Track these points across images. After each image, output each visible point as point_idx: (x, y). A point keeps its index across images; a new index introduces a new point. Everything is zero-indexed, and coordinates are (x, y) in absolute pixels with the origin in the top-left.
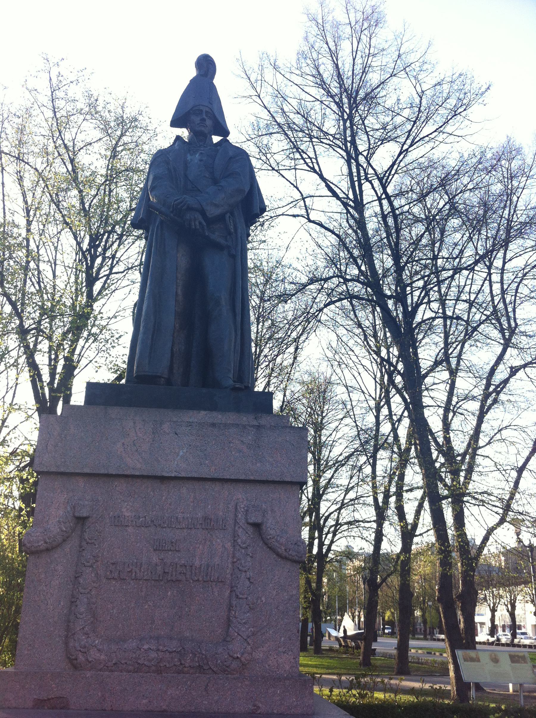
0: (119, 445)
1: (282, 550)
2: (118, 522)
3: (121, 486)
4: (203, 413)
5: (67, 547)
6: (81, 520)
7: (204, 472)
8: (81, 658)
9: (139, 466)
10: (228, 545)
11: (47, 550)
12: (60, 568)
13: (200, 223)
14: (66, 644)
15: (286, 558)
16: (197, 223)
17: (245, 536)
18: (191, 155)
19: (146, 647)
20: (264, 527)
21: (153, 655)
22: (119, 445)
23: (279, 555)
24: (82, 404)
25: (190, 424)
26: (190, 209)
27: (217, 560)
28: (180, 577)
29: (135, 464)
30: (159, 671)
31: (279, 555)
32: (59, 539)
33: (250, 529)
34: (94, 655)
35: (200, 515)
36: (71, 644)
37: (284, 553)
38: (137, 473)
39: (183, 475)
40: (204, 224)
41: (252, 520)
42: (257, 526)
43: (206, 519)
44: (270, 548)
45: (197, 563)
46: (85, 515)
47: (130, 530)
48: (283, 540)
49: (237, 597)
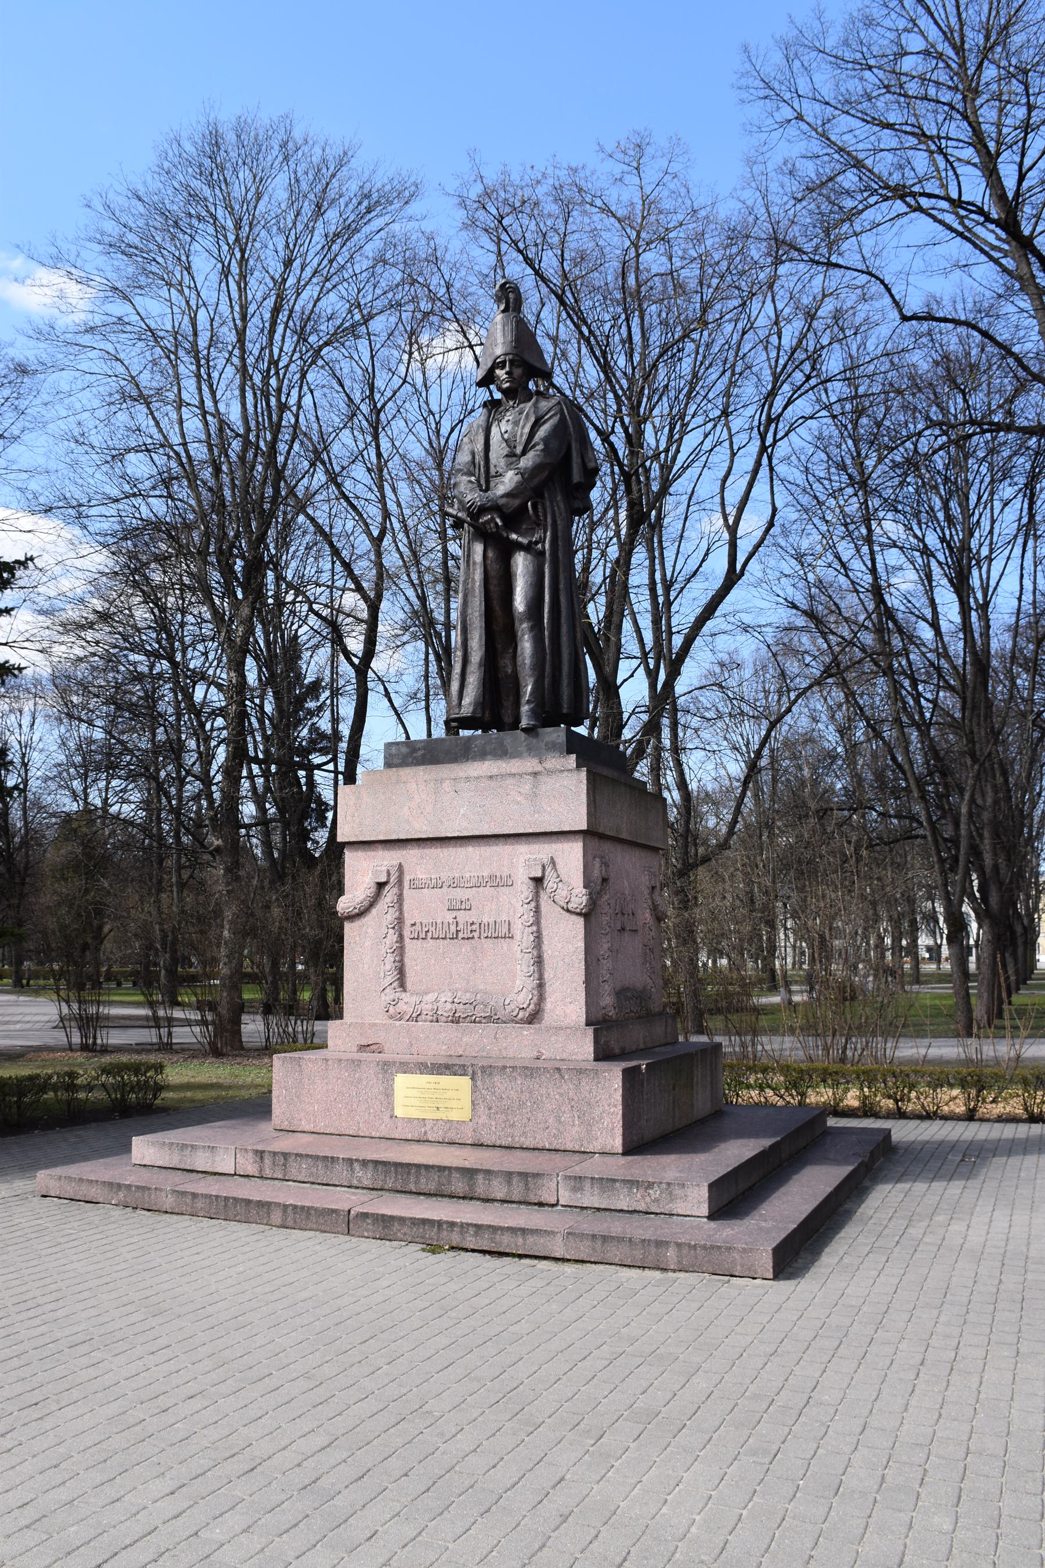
0: (406, 809)
4: (487, 763)
6: (381, 886)
21: (449, 1006)
22: (406, 809)
27: (504, 918)
33: (531, 884)
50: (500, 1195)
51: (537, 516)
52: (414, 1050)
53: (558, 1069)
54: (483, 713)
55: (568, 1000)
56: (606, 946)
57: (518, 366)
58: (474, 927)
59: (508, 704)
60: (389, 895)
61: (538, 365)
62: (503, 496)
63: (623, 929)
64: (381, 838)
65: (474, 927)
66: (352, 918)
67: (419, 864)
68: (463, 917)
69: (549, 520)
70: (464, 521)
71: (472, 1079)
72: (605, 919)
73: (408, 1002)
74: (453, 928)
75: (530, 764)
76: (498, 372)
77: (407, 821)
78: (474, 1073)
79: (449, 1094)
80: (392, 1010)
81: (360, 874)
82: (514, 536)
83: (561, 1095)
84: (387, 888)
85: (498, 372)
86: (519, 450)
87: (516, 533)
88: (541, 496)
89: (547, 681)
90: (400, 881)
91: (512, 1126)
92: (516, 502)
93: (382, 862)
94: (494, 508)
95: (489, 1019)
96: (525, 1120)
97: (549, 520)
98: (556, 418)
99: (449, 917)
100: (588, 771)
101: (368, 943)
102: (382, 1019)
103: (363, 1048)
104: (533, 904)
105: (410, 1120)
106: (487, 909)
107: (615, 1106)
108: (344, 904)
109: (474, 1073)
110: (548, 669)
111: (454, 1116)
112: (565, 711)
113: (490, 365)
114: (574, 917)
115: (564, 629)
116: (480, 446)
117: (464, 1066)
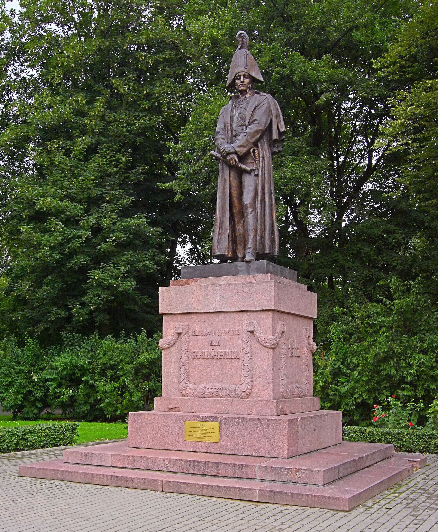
1: (263, 343)
3: (195, 317)
5: (176, 346)
6: (179, 334)
8: (184, 392)
10: (240, 342)
11: (169, 348)
12: (174, 355)
13: (235, 160)
15: (265, 347)
16: (234, 161)
17: (247, 337)
21: (210, 390)
23: (263, 345)
24: (160, 288)
25: (220, 285)
26: (228, 154)
27: (236, 349)
28: (221, 357)
31: (263, 345)
32: (172, 343)
33: (249, 334)
34: (188, 390)
37: (264, 344)
40: (237, 160)
42: (252, 332)
43: (230, 330)
45: (228, 351)
47: (200, 337)
48: (263, 338)
50: (230, 475)
51: (255, 156)
52: (194, 410)
53: (259, 419)
54: (228, 253)
55: (265, 388)
56: (283, 363)
57: (247, 78)
58: (222, 354)
59: (240, 248)
60: (183, 338)
62: (238, 147)
63: (293, 356)
65: (222, 354)
66: (165, 349)
67: (197, 325)
68: (216, 348)
69: (261, 159)
70: (220, 159)
71: (220, 423)
72: (283, 351)
74: (212, 354)
75: (249, 278)
76: (237, 81)
77: (192, 304)
78: (221, 421)
79: (209, 431)
80: (184, 392)
81: (169, 328)
82: (243, 166)
83: (260, 431)
84: (182, 335)
85: (237, 81)
86: (247, 123)
87: (244, 164)
88: (257, 146)
89: (258, 238)
90: (188, 332)
91: (238, 445)
92: (245, 150)
93: (180, 324)
96: (244, 442)
97: (261, 159)
98: (264, 107)
99: (211, 349)
100: (275, 282)
102: (179, 397)
106: (228, 345)
107: (284, 436)
108: (162, 342)
109: (221, 421)
110: (259, 232)
111: (211, 440)
112: (267, 252)
113: (233, 77)
114: (267, 350)
115: (267, 212)
117: (216, 417)
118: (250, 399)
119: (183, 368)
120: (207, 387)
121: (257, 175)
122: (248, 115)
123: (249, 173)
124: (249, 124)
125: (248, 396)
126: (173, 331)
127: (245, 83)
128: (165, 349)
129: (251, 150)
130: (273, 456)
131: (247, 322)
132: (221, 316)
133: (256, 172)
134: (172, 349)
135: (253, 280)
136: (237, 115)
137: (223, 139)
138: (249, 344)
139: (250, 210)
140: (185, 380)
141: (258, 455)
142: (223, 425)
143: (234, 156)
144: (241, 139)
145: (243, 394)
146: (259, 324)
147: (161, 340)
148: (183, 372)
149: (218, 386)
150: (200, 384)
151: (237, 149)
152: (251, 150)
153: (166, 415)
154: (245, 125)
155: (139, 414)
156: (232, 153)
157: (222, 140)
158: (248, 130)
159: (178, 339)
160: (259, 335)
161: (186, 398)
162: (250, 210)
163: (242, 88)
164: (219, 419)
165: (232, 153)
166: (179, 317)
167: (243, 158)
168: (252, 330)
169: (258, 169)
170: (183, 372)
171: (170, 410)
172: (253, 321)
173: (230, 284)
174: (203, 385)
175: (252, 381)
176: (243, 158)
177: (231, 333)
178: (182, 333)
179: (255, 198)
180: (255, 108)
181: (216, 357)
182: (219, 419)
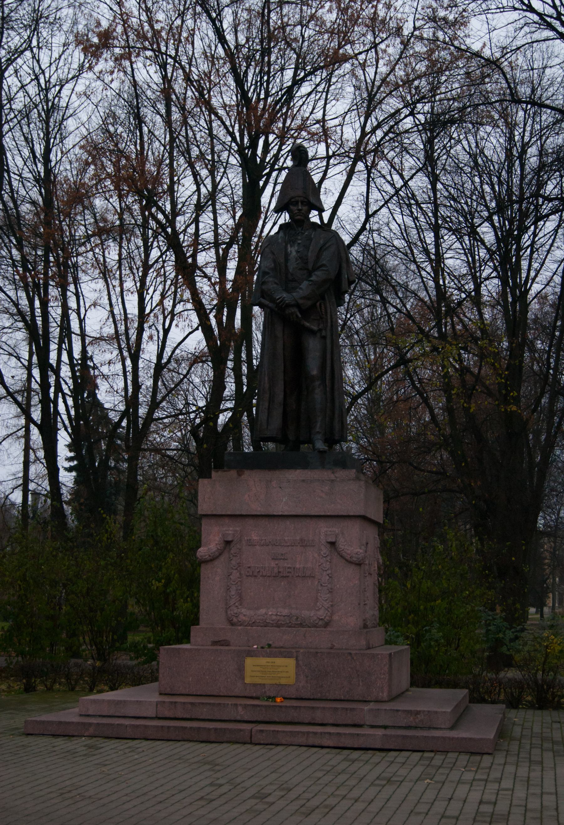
0: (246, 496)
1: (348, 557)
2: (250, 543)
3: (251, 521)
4: (298, 471)
5: (222, 558)
6: (228, 543)
7: (299, 512)
8: (235, 620)
9: (259, 509)
10: (316, 555)
12: (219, 570)
13: (297, 316)
14: (226, 612)
16: (294, 316)
17: (325, 550)
18: (291, 246)
19: (270, 613)
20: (337, 544)
21: (274, 617)
22: (246, 496)
23: (347, 560)
26: (288, 306)
27: (309, 565)
29: (257, 508)
30: (278, 626)
31: (347, 560)
32: (217, 554)
33: (329, 545)
34: (242, 618)
35: (298, 538)
36: (229, 613)
37: (349, 559)
38: (259, 513)
39: (286, 513)
40: (300, 316)
41: (330, 540)
42: (333, 544)
43: (302, 540)
44: (341, 556)
45: (298, 566)
46: (230, 539)
47: (258, 547)
48: (349, 552)
49: (321, 585)
53: (350, 654)
58: (289, 570)
61: (318, 205)
62: (301, 298)
64: (229, 513)
65: (289, 570)
66: (206, 562)
71: (297, 659)
73: (245, 614)
75: (326, 474)
82: (307, 324)
86: (310, 267)
88: (323, 298)
92: (309, 303)
93: (230, 529)
94: (298, 306)
95: (301, 625)
99: (273, 564)
101: (217, 578)
103: (215, 643)
104: (328, 558)
105: (255, 685)
107: (384, 674)
108: (202, 552)
111: (283, 681)
116: (282, 260)
118: (329, 629)
119: (234, 588)
120: (270, 613)
121: (324, 338)
122: (311, 256)
123: (313, 333)
124: (315, 269)
125: (327, 625)
126: (217, 538)
127: (303, 212)
128: (206, 562)
129: (318, 304)
130: (369, 699)
131: (325, 531)
132: (288, 522)
133: (324, 333)
134: (216, 563)
135: (332, 477)
136: (294, 253)
137: (276, 283)
138: (328, 558)
139: (317, 383)
140: (237, 604)
141: (349, 698)
142: (300, 662)
143: (295, 310)
144: (305, 288)
145: (320, 623)
146: (343, 534)
147: (199, 550)
148: (233, 593)
149: (285, 612)
150: (258, 608)
151: (301, 302)
152: (318, 304)
153: (217, 650)
154: (308, 269)
155: (176, 649)
156: (292, 306)
157: (275, 286)
158: (313, 278)
159: (225, 548)
160: (343, 547)
161: (240, 628)
162: (317, 383)
163: (299, 217)
164: (295, 654)
165: (292, 306)
166: (227, 520)
167: (306, 312)
168: (333, 540)
169: (326, 330)
170: (233, 593)
171: (215, 643)
172: (334, 529)
173: (303, 481)
174: (263, 611)
175: (332, 606)
176: (306, 312)
177: (304, 544)
178: (231, 541)
179: (323, 368)
180: (321, 248)
181: (281, 575)
182: (295, 654)
